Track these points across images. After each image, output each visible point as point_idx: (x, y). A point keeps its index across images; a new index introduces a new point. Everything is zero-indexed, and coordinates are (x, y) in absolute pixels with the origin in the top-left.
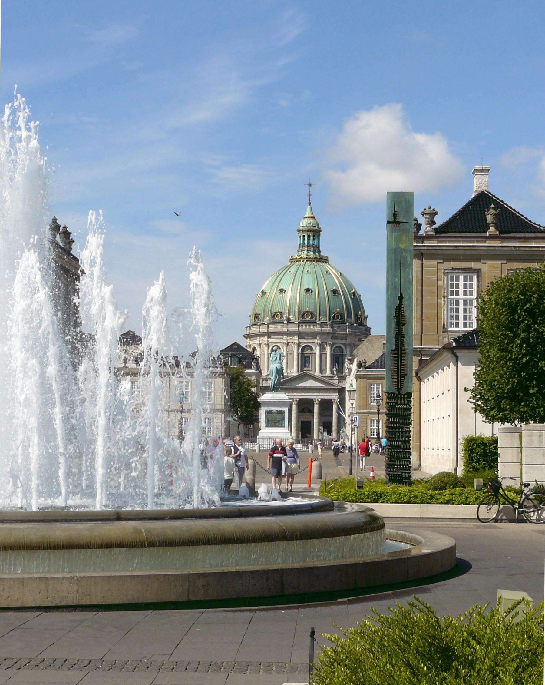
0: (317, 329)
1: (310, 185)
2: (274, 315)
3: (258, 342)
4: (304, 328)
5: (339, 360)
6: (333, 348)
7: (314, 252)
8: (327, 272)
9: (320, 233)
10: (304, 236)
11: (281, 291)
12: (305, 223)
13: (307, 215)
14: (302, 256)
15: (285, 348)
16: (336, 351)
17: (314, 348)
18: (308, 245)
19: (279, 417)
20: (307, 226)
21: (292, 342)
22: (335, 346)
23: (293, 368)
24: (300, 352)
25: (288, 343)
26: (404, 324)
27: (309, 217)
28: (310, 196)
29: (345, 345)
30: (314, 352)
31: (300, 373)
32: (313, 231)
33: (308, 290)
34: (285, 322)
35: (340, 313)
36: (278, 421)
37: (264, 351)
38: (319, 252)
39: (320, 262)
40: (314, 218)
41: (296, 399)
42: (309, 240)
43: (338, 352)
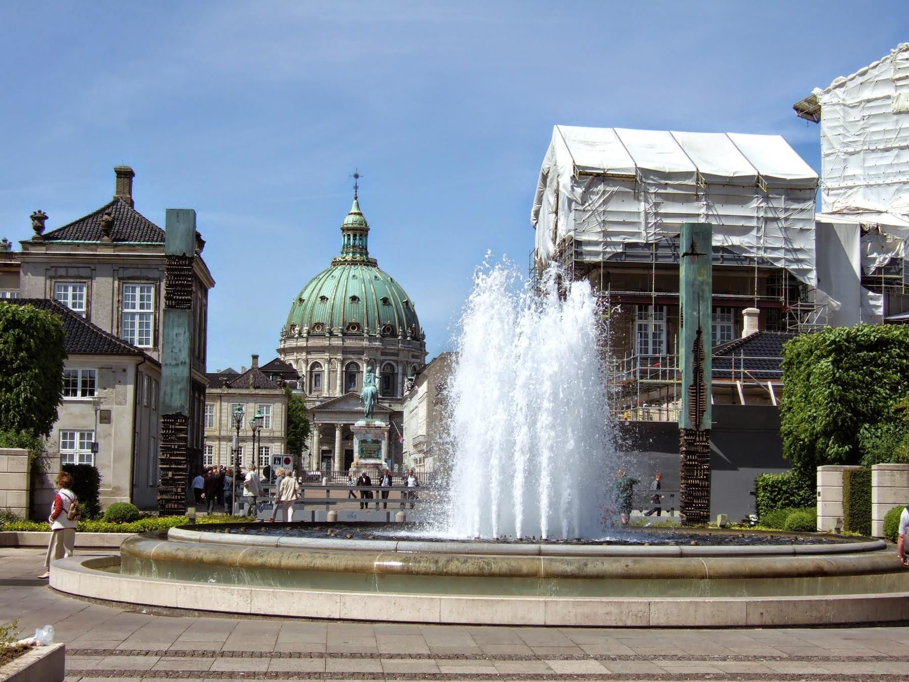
0: (365, 343)
1: (356, 176)
2: (315, 326)
3: (295, 358)
4: (349, 343)
5: (389, 379)
6: (383, 367)
7: (361, 254)
8: (376, 277)
9: (367, 232)
10: (349, 235)
12: (349, 220)
13: (352, 211)
14: (347, 258)
15: (326, 365)
16: (386, 370)
18: (354, 246)
19: (375, 446)
20: (352, 224)
22: (385, 363)
23: (336, 389)
25: (331, 359)
26: (702, 359)
27: (355, 214)
28: (356, 189)
29: (397, 362)
30: (361, 370)
31: (344, 395)
32: (360, 230)
33: (354, 298)
34: (327, 335)
36: (374, 451)
37: (301, 369)
38: (367, 254)
39: (367, 265)
41: (340, 424)
42: (355, 239)
43: (389, 371)
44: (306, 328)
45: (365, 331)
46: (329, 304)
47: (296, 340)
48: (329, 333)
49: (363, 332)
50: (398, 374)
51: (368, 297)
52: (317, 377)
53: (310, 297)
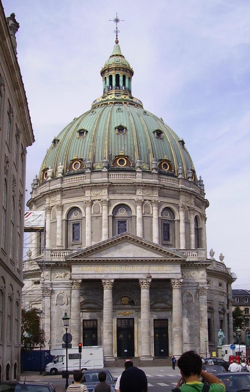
1: (117, 21)
4: (115, 178)
5: (168, 228)
6: (161, 210)
10: (111, 77)
11: (80, 133)
15: (88, 209)
17: (132, 207)
21: (99, 200)
22: (163, 207)
24: (111, 213)
27: (117, 55)
30: (134, 214)
32: (123, 70)
33: (121, 129)
34: (89, 171)
35: (168, 161)
37: (55, 218)
40: (124, 57)
43: (168, 217)
44: (60, 168)
45: (137, 165)
46: (88, 138)
47: (48, 183)
48: (90, 169)
49: (134, 166)
50: (179, 221)
51: (138, 128)
52: (76, 227)
53: (65, 136)
